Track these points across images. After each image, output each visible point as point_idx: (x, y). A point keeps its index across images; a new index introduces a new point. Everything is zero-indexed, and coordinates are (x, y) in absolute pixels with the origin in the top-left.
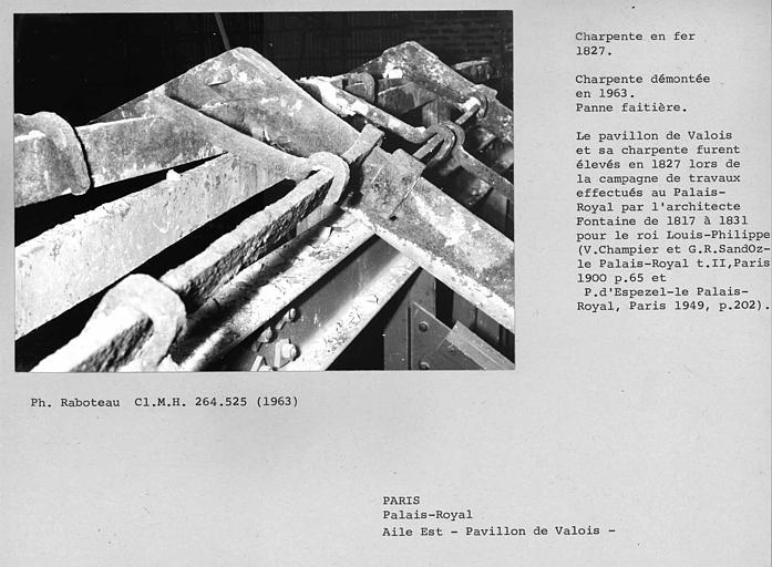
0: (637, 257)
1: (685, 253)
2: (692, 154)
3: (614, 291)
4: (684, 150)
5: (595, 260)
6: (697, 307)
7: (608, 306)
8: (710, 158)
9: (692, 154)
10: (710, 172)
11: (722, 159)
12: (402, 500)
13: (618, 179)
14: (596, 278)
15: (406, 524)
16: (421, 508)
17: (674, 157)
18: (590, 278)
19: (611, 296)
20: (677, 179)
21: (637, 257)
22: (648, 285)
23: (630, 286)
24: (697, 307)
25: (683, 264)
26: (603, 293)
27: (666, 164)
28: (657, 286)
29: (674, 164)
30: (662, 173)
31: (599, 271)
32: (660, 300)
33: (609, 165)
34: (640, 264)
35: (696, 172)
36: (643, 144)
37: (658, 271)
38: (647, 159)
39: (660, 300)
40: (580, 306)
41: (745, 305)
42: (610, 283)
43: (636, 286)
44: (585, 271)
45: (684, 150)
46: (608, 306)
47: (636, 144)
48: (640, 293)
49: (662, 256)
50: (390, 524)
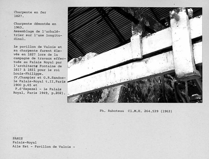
0: (30, 80)
1: (42, 79)
2: (39, 52)
3: (23, 89)
4: (37, 51)
5: (18, 80)
6: (46, 93)
7: (21, 93)
8: (44, 53)
9: (39, 52)
10: (43, 57)
11: (47, 53)
12: (18, 138)
13: (19, 58)
14: (18, 85)
15: (19, 145)
16: (23, 141)
17: (34, 52)
18: (17, 85)
19: (22, 90)
20: (35, 58)
21: (30, 80)
22: (32, 87)
23: (28, 87)
24: (46, 93)
25: (42, 81)
26: (20, 89)
27: (32, 54)
28: (35, 87)
29: (34, 54)
30: (31, 57)
31: (20, 83)
32: (35, 91)
33: (16, 54)
34: (30, 81)
35: (40, 57)
36: (25, 49)
37: (35, 83)
38: (26, 53)
39: (35, 91)
40: (14, 93)
41: (58, 93)
42: (22, 86)
43: (29, 87)
44: (15, 83)
45: (37, 51)
46: (21, 93)
47: (24, 49)
48: (30, 89)
49: (36, 79)
50: (15, 144)
